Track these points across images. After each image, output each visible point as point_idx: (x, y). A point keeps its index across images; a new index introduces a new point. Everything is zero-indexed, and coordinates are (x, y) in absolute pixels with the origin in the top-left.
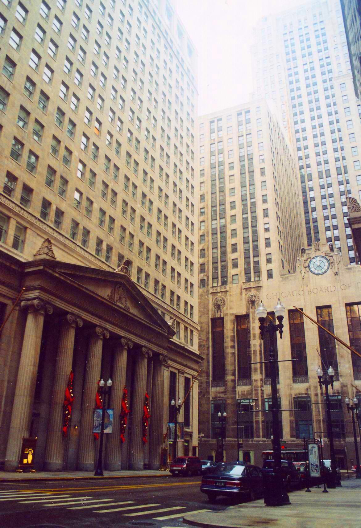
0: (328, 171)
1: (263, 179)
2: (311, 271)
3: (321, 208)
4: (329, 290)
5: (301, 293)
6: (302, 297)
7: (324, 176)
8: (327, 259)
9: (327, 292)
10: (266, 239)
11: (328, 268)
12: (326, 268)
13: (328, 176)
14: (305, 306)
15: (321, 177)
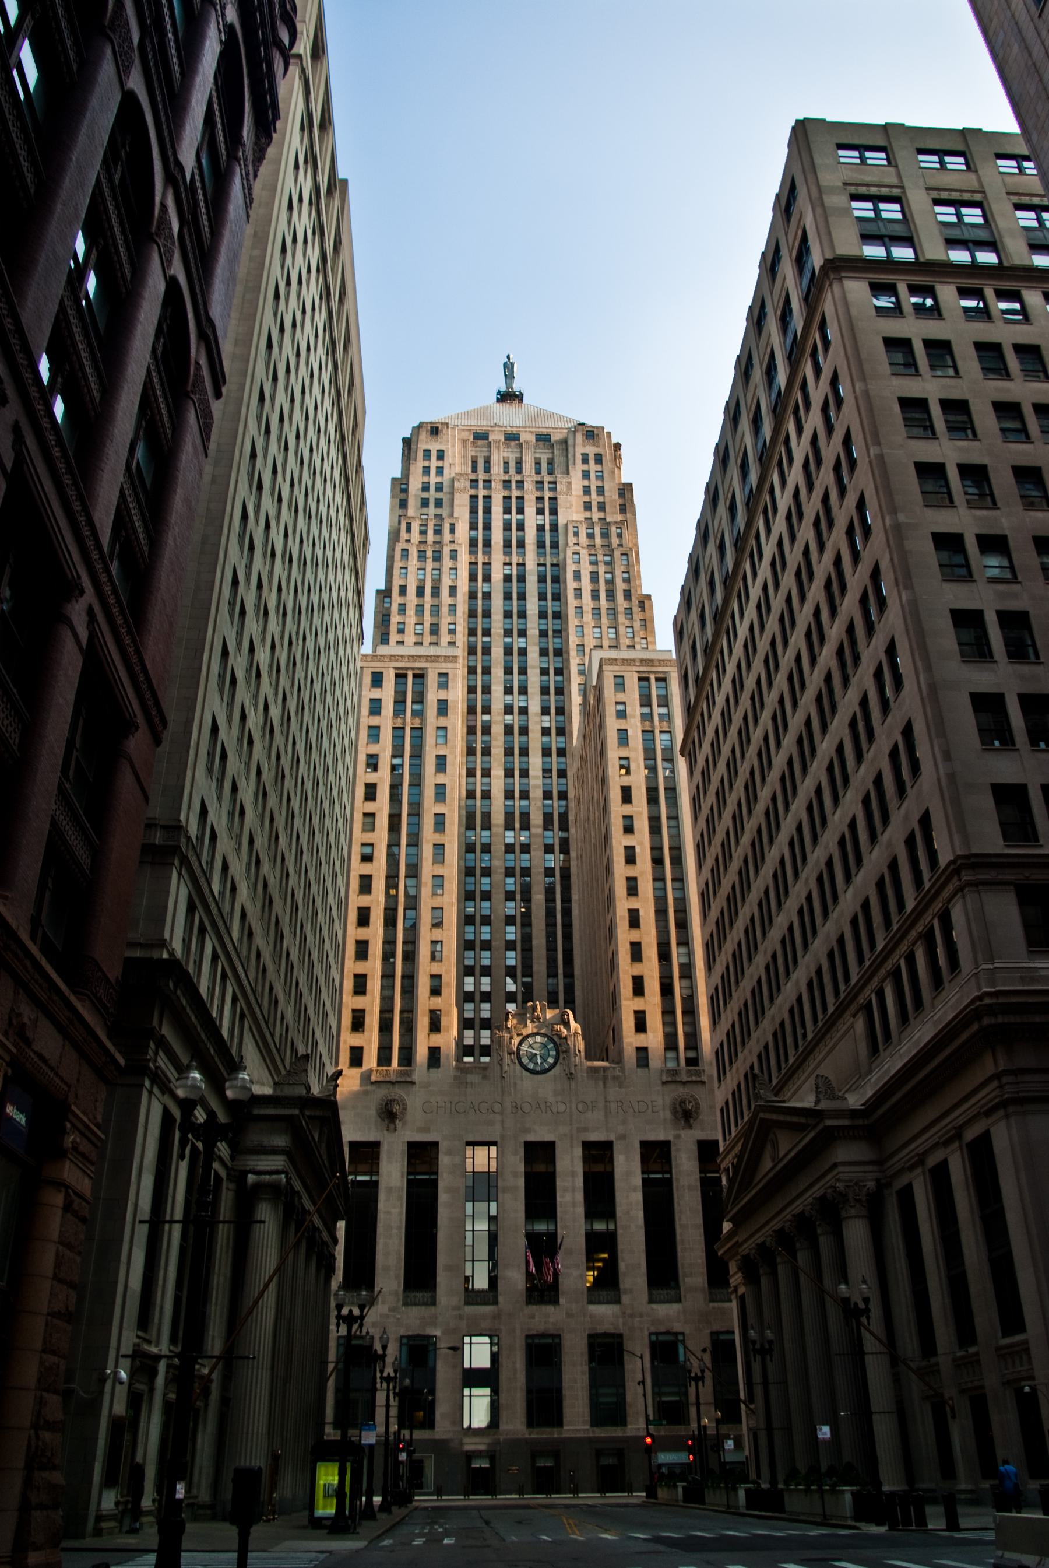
0: (525, 816)
1: (438, 838)
2: (521, 1063)
3: (502, 896)
4: (555, 1110)
5: (497, 1107)
6: (498, 1117)
7: (517, 826)
8: (555, 1043)
9: (549, 1112)
10: (432, 976)
11: (555, 1063)
12: (551, 1060)
13: (526, 826)
14: (503, 1137)
15: (509, 826)
